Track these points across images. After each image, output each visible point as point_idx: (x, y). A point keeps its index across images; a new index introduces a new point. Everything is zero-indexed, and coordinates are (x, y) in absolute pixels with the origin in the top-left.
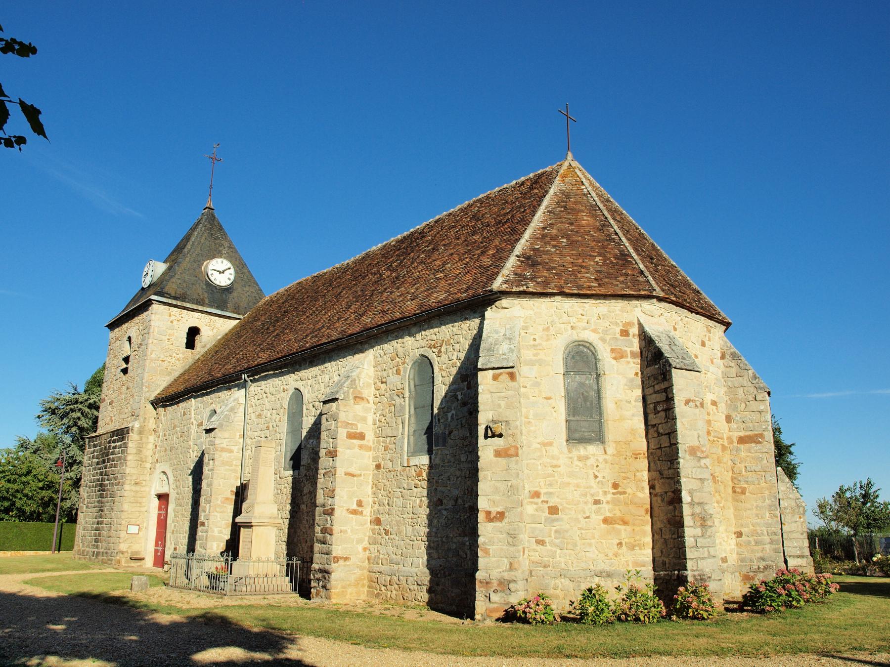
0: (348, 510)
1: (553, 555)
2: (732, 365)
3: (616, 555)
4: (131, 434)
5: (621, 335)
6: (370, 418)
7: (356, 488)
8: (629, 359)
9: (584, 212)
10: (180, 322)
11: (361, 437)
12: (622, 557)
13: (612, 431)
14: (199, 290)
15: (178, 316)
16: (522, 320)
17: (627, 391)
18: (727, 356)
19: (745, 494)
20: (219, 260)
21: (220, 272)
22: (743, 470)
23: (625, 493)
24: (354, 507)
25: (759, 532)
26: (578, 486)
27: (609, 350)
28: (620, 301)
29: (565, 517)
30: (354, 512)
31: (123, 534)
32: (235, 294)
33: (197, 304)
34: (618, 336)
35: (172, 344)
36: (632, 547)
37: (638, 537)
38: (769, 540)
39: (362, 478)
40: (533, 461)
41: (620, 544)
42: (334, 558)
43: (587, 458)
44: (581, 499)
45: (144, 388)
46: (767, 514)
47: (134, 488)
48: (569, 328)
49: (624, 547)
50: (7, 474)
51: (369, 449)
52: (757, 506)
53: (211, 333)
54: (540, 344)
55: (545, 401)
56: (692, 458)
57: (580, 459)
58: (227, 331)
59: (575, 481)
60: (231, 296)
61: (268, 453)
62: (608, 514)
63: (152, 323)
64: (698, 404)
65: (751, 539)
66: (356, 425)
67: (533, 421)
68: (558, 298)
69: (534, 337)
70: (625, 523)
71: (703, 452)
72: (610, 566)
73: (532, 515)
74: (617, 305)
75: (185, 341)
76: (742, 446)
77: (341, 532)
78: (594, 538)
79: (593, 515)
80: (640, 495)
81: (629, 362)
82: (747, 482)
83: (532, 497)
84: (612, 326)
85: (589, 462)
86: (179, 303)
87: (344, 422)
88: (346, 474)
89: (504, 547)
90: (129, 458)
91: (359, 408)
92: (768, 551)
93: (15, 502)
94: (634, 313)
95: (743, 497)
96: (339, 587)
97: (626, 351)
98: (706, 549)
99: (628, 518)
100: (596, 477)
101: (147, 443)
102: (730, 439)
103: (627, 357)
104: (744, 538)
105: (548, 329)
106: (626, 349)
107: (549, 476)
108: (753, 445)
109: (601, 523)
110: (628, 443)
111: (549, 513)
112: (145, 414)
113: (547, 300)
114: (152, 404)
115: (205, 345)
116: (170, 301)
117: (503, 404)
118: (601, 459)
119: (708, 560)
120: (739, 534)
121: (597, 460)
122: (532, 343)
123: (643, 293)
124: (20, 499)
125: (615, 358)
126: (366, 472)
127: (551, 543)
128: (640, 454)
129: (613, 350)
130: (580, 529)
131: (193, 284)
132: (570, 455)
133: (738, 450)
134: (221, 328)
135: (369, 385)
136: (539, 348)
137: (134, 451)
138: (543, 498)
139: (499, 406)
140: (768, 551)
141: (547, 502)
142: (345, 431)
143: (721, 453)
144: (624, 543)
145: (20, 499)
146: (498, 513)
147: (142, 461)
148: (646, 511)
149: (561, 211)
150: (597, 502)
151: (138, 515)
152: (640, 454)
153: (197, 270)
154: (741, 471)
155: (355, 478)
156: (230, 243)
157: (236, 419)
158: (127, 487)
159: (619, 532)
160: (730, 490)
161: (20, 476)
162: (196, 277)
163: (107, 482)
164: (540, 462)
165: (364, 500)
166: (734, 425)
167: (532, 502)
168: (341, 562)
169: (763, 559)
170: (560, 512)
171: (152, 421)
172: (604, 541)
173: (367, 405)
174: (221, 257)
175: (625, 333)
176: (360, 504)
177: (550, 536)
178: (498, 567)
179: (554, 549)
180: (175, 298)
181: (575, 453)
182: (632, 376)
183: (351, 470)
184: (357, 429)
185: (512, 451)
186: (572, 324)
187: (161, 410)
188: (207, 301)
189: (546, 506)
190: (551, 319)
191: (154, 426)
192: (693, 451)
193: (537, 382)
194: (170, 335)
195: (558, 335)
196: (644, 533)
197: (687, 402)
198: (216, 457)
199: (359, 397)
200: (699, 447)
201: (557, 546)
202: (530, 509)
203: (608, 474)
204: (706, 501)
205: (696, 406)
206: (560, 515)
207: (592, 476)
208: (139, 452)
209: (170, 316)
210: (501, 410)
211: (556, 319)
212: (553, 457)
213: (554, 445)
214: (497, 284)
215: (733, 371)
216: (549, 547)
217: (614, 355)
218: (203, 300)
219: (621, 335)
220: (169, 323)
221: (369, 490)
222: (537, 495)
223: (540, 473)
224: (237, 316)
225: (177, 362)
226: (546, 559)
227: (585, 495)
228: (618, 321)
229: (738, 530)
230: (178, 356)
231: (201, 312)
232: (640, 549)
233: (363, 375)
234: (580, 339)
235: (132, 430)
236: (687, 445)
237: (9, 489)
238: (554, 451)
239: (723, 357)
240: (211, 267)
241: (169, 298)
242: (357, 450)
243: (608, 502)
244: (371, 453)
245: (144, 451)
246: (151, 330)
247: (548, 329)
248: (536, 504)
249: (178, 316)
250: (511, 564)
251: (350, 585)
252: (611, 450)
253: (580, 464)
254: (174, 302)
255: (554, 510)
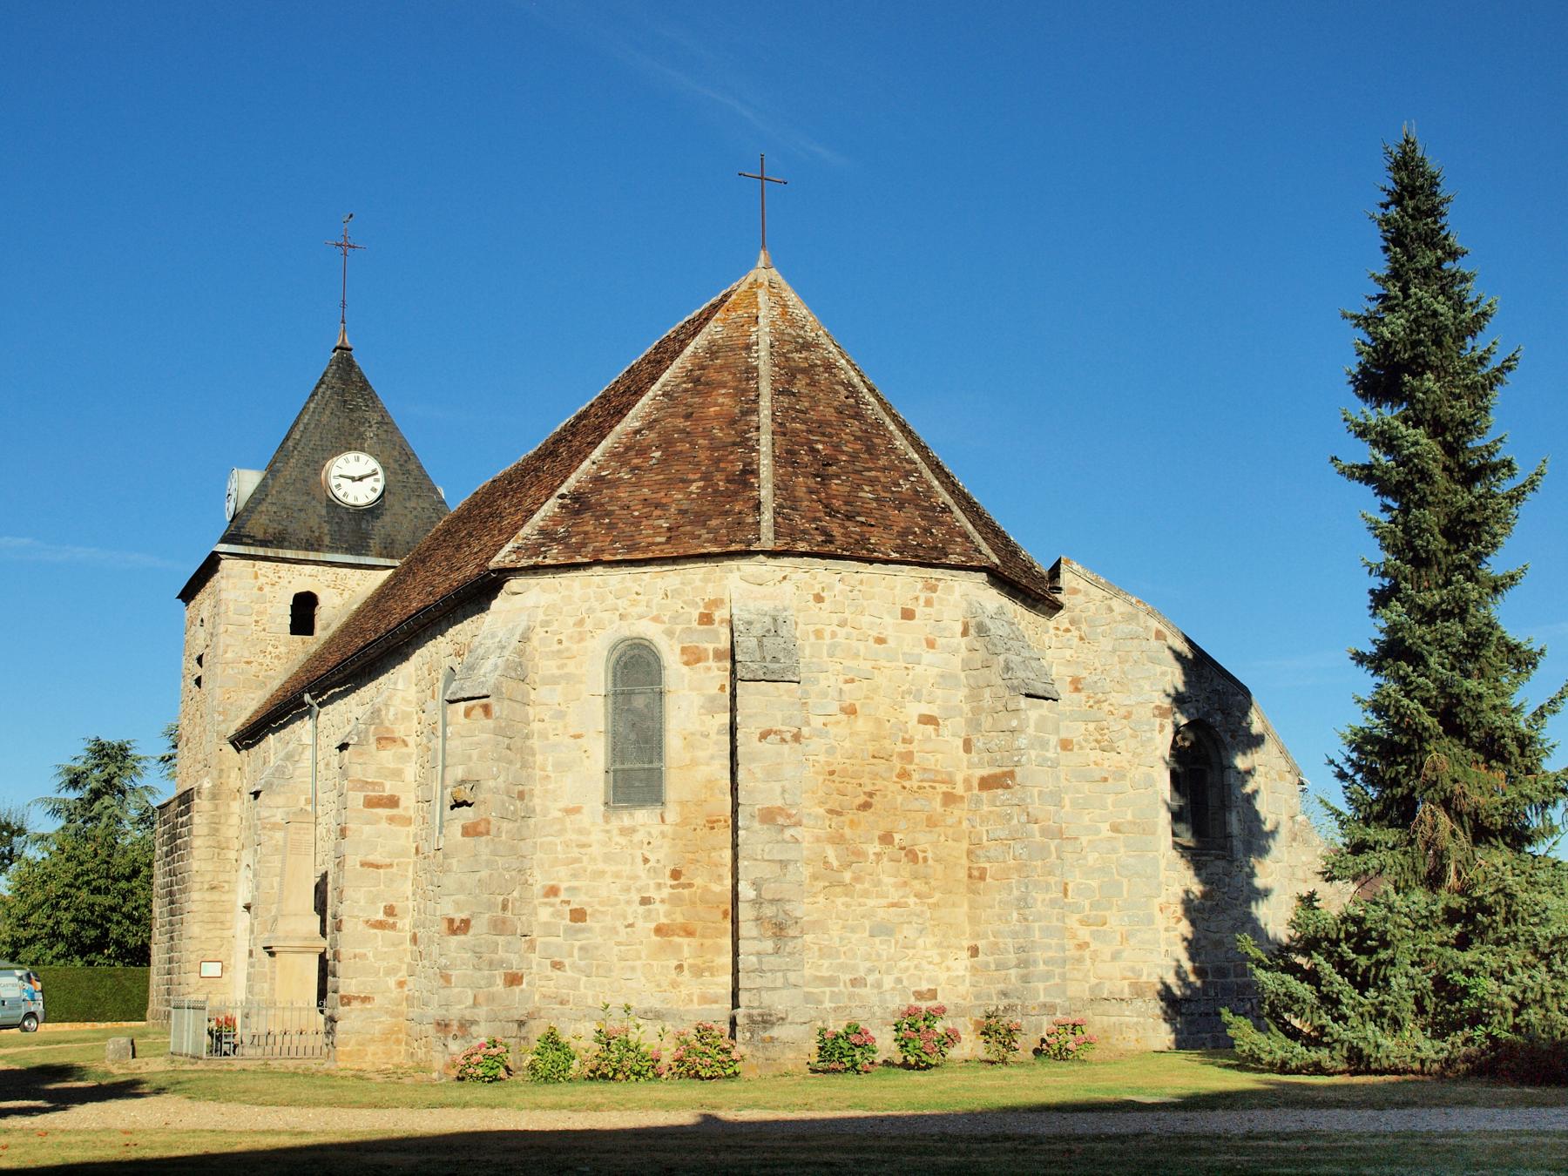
0: (367, 922)
1: (575, 987)
2: (977, 645)
3: (674, 985)
4: (197, 801)
5: (699, 624)
6: (411, 771)
7: (382, 886)
8: (711, 663)
9: (725, 387)
10: (277, 587)
11: (393, 802)
12: (682, 988)
13: (674, 787)
14: (315, 519)
15: (271, 575)
16: (541, 611)
17: (703, 717)
18: (972, 631)
19: (984, 879)
20: (351, 456)
21: (353, 479)
22: (985, 838)
23: (690, 885)
24: (381, 916)
25: (1002, 946)
26: (617, 875)
27: (678, 651)
28: (702, 564)
29: (597, 926)
30: (380, 925)
31: (193, 978)
32: (387, 518)
33: (307, 550)
34: (695, 624)
35: (264, 630)
36: (698, 972)
37: (709, 957)
38: (1015, 962)
39: (395, 870)
40: (550, 838)
41: (680, 967)
42: (342, 997)
43: (633, 830)
44: (621, 897)
45: (216, 715)
46: (1015, 915)
47: (208, 896)
48: (616, 617)
49: (686, 972)
50: (92, 876)
51: (408, 821)
52: (1000, 902)
53: (338, 601)
54: (568, 649)
55: (572, 740)
56: (765, 827)
57: (625, 831)
58: (369, 593)
59: (614, 868)
60: (378, 523)
61: (302, 832)
62: (664, 920)
63: (224, 595)
64: (788, 737)
65: (991, 959)
66: (382, 784)
67: (552, 775)
68: (599, 569)
69: (561, 637)
70: (690, 933)
71: (789, 816)
72: (663, 1001)
73: (546, 924)
74: (696, 572)
75: (289, 620)
76: (985, 794)
77: (355, 957)
78: (640, 958)
79: (640, 924)
80: (716, 888)
81: (709, 669)
82: (989, 860)
83: (547, 895)
84: (687, 609)
85: (637, 838)
86: (270, 552)
87: (359, 780)
88: (363, 865)
89: (469, 972)
90: (197, 843)
91: (387, 756)
92: (1013, 980)
93: (108, 930)
94: (726, 582)
95: (982, 885)
96: (353, 1042)
97: (706, 650)
98: (779, 974)
99: (698, 926)
100: (646, 860)
101: (228, 815)
102: (967, 781)
103: (707, 659)
104: (981, 957)
105: (581, 623)
106: (706, 645)
107: (577, 860)
108: (1000, 791)
109: (652, 933)
110: (700, 803)
111: (571, 920)
112: (220, 761)
113: (581, 573)
114: (232, 743)
115: (329, 625)
116: (252, 550)
117: (475, 754)
118: (655, 831)
119: (785, 992)
120: (974, 951)
121: (649, 833)
122: (556, 647)
123: (734, 547)
124: (119, 923)
125: (687, 663)
126: (402, 860)
127: (573, 966)
128: (720, 821)
129: (684, 650)
130: (619, 944)
131: (300, 510)
132: (608, 827)
133: (979, 801)
134: (358, 589)
135: (406, 717)
136: (566, 654)
137: (205, 831)
138: (563, 896)
139: (470, 757)
140: (1013, 980)
141: (568, 902)
142: (361, 795)
143: (940, 809)
144: (686, 966)
145: (119, 923)
146: (462, 921)
147: (220, 848)
148: (725, 914)
149: (686, 390)
150: (645, 901)
151: (220, 943)
152: (720, 821)
153: (311, 481)
154: (981, 839)
155: (381, 871)
156: (384, 414)
157: (297, 773)
158: (195, 896)
159: (678, 949)
160: (963, 874)
161: (116, 880)
162: (309, 494)
163: (176, 887)
164: (562, 839)
165: (399, 906)
166: (975, 757)
167: (546, 904)
168: (356, 1005)
169: (1005, 994)
170: (588, 918)
171: (234, 773)
172: (654, 963)
173: (405, 750)
174: (363, 450)
175: (706, 619)
176: (390, 911)
177: (571, 955)
178: (460, 1002)
179: (577, 976)
180: (264, 543)
181: (615, 824)
182: (715, 691)
183: (374, 858)
184: (384, 791)
185: (482, 828)
186: (621, 611)
187: (244, 752)
188: (327, 540)
189: (567, 908)
190: (587, 605)
191: (239, 785)
192: (768, 816)
193: (561, 711)
194: (259, 613)
195: (599, 631)
196: (718, 950)
197: (764, 736)
198: (264, 838)
199: (386, 739)
200: (783, 809)
201: (581, 971)
202: (544, 914)
203: (663, 855)
204: (787, 897)
205: (783, 740)
206: (589, 922)
207: (639, 860)
208: (214, 831)
209: (256, 577)
210: (471, 764)
211: (596, 605)
212: (581, 831)
213: (584, 811)
214: (503, 558)
215: (978, 657)
216: (569, 973)
217: (685, 658)
218: (319, 539)
219: (699, 624)
220: (255, 590)
221: (408, 888)
222: (553, 891)
223: (560, 856)
224: (388, 562)
225: (276, 661)
226: (564, 991)
227: (628, 890)
228: (698, 599)
229: (973, 943)
230: (277, 651)
231: (316, 563)
232: (712, 975)
233: (397, 701)
234: (634, 635)
235: (198, 792)
236: (757, 807)
237: (93, 904)
238: (584, 819)
239: (965, 633)
240: (335, 471)
241: (252, 545)
242: (384, 825)
243: (663, 901)
244: (412, 829)
245: (224, 829)
246: (223, 608)
247: (581, 623)
248: (552, 905)
249: (271, 575)
250: (475, 997)
251: (372, 1040)
252: (672, 815)
253: (623, 841)
254: (261, 551)
255: (578, 915)
